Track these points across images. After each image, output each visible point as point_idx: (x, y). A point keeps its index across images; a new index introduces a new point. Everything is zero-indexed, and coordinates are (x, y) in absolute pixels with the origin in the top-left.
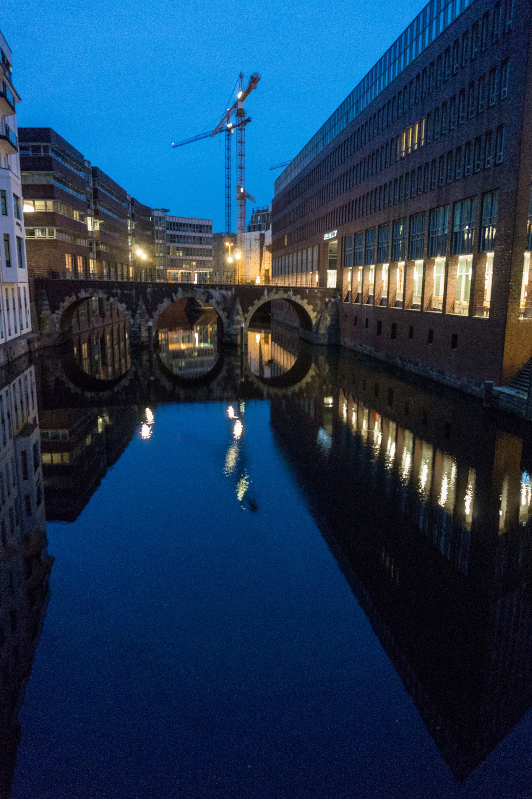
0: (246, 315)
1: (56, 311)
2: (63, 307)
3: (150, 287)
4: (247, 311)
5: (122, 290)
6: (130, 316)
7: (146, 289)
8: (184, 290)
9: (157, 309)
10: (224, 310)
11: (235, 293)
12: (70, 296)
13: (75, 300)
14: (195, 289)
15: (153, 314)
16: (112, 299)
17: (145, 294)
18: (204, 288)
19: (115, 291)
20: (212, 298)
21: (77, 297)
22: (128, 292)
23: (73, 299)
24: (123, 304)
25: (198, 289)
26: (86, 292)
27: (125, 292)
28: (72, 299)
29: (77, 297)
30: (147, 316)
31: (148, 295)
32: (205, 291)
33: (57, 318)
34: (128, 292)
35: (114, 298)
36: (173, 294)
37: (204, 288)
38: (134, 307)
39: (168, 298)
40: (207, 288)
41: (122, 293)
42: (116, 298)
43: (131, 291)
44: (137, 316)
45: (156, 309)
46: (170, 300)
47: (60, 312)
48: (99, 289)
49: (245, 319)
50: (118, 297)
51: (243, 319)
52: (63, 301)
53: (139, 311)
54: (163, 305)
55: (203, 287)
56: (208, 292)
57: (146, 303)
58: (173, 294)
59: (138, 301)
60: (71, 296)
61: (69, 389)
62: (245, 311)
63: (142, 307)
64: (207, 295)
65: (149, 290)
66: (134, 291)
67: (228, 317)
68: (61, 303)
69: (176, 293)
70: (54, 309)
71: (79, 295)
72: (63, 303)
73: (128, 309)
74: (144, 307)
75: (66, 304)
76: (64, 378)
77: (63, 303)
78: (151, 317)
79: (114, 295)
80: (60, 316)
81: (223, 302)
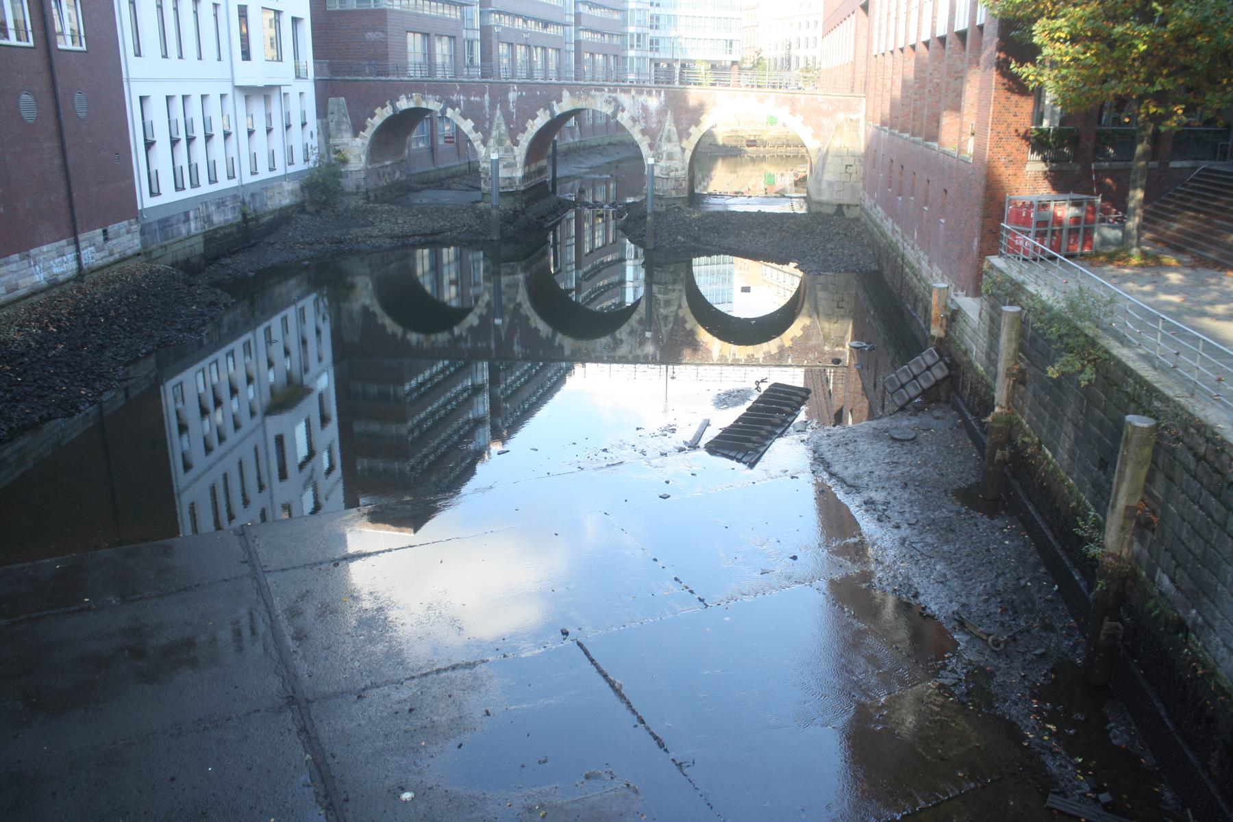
0: (685, 143)
1: (361, 133)
2: (373, 125)
3: (514, 90)
4: (689, 135)
5: (468, 95)
6: (479, 142)
7: (507, 91)
8: (572, 94)
9: (527, 128)
10: (644, 132)
11: (665, 101)
12: (384, 106)
13: (391, 113)
14: (593, 92)
15: (518, 138)
16: (450, 113)
17: (505, 102)
18: (610, 91)
19: (455, 98)
20: (623, 110)
21: (394, 108)
22: (478, 99)
23: (388, 112)
24: (469, 120)
25: (598, 93)
26: (407, 98)
27: (472, 98)
28: (387, 112)
29: (394, 108)
30: (508, 142)
31: (511, 105)
32: (610, 97)
33: (363, 144)
34: (478, 99)
35: (454, 109)
36: (554, 102)
37: (610, 91)
38: (487, 126)
39: (545, 109)
40: (615, 91)
41: (468, 102)
42: (457, 109)
43: (482, 96)
44: (491, 142)
45: (524, 130)
46: (548, 112)
47: (368, 134)
48: (428, 94)
49: (683, 150)
50: (460, 108)
51: (678, 149)
52: (373, 116)
53: (494, 133)
54: (535, 121)
55: (606, 89)
56: (615, 100)
57: (507, 116)
58: (554, 102)
59: (492, 116)
60: (386, 106)
61: (383, 326)
62: (683, 134)
63: (500, 128)
64: (613, 104)
65: (512, 96)
66: (487, 97)
67: (651, 146)
68: (369, 119)
69: (559, 100)
70: (358, 129)
71: (398, 104)
72: (372, 118)
73: (476, 129)
74: (503, 127)
75: (377, 121)
76: (377, 308)
77: (372, 118)
78: (516, 143)
79: (453, 106)
80: (367, 142)
81: (644, 118)
